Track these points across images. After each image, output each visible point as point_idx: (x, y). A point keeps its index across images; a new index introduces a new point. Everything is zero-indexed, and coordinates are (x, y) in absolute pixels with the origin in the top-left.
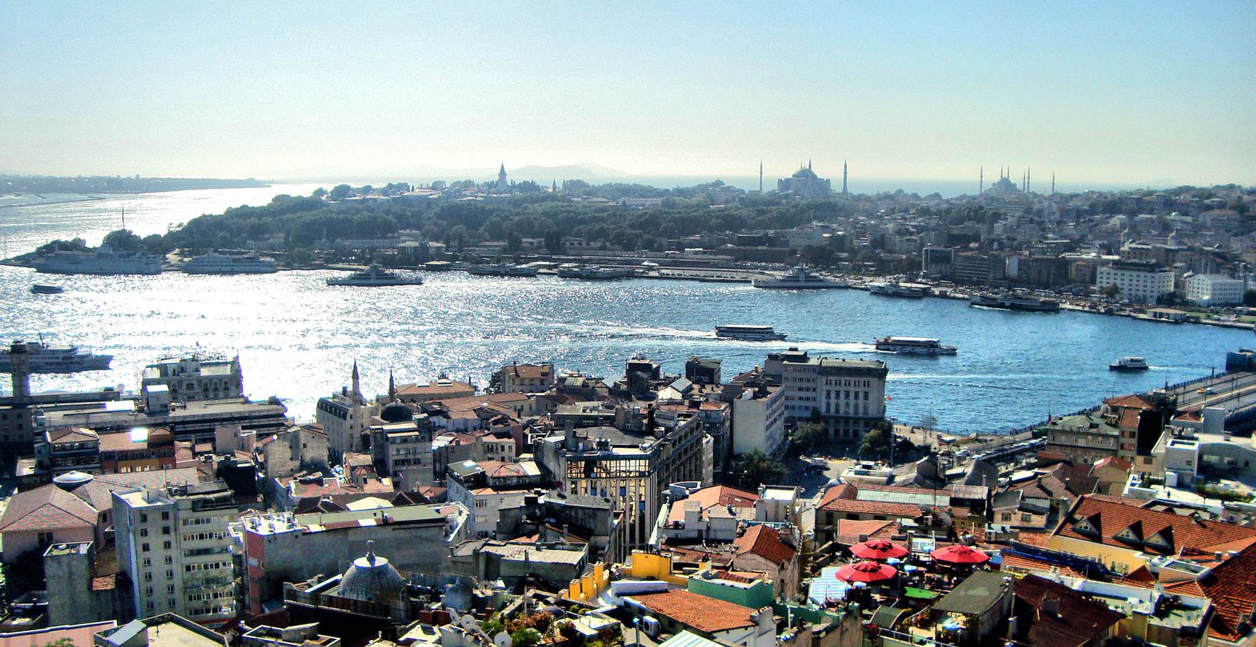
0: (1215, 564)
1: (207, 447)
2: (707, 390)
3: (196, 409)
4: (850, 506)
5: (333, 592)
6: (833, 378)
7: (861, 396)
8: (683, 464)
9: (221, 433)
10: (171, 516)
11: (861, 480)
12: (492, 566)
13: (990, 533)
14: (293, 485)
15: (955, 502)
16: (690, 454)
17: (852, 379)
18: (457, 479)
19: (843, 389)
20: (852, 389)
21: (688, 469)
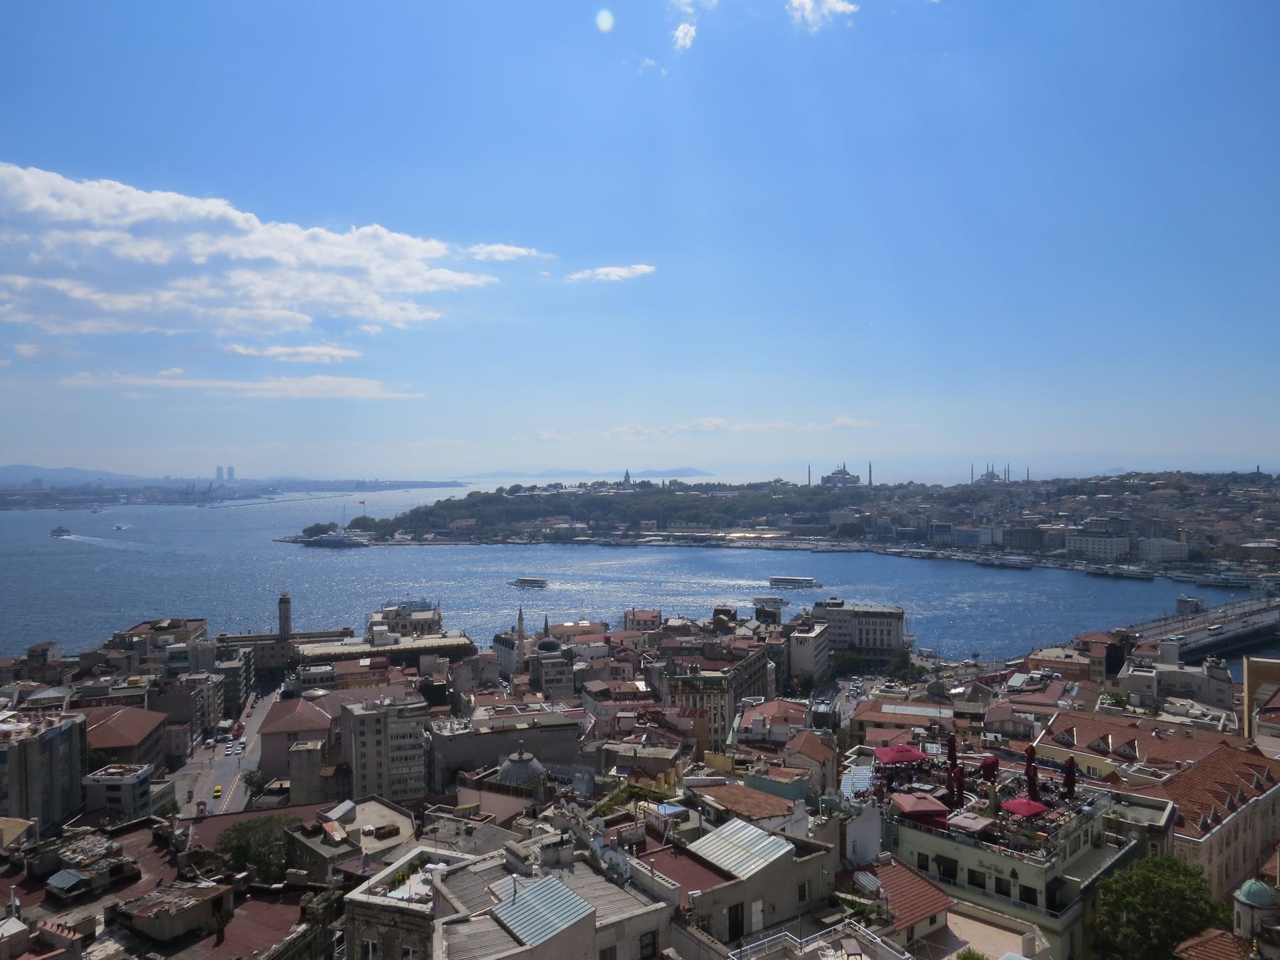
0: (1176, 772)
1: (414, 670)
2: (771, 628)
3: (407, 643)
4: (875, 717)
5: (492, 779)
6: (863, 620)
7: (885, 633)
8: (754, 683)
9: (425, 660)
10: (382, 720)
11: (885, 697)
12: (611, 758)
13: (985, 741)
14: (473, 698)
15: (958, 715)
16: (758, 676)
17: (878, 620)
18: (589, 693)
19: (871, 627)
20: (878, 628)
21: (756, 687)
